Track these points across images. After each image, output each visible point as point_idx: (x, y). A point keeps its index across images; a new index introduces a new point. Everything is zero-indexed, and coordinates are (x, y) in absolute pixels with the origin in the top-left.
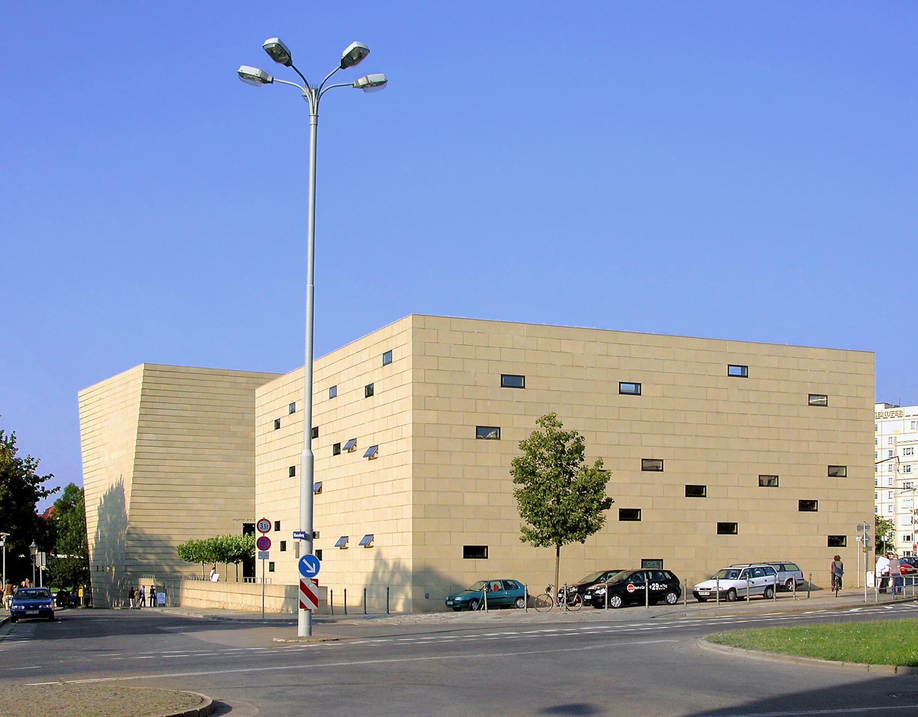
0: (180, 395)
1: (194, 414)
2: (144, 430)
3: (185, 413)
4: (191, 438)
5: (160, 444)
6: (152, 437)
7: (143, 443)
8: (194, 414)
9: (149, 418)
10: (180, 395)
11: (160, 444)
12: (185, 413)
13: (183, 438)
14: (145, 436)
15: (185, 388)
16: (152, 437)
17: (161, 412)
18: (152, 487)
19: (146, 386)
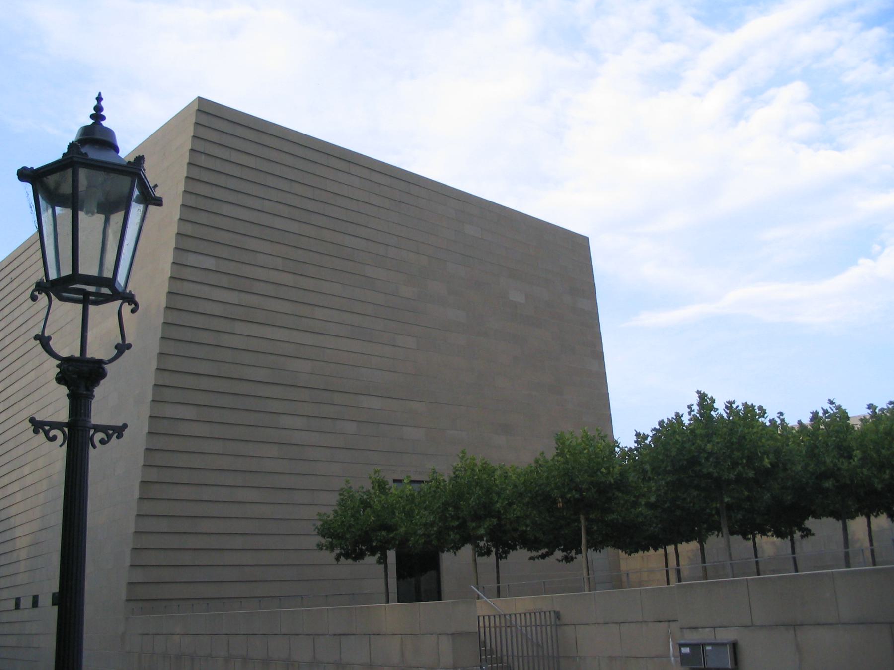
0: (271, 181)
1: (294, 227)
2: (190, 244)
3: (278, 223)
4: (288, 279)
5: (224, 281)
6: (209, 263)
7: (187, 273)
8: (294, 227)
9: (203, 218)
10: (271, 181)
11: (224, 281)
12: (278, 223)
13: (273, 276)
14: (191, 259)
15: (277, 170)
16: (209, 263)
17: (226, 210)
18: (205, 383)
19: (200, 146)
